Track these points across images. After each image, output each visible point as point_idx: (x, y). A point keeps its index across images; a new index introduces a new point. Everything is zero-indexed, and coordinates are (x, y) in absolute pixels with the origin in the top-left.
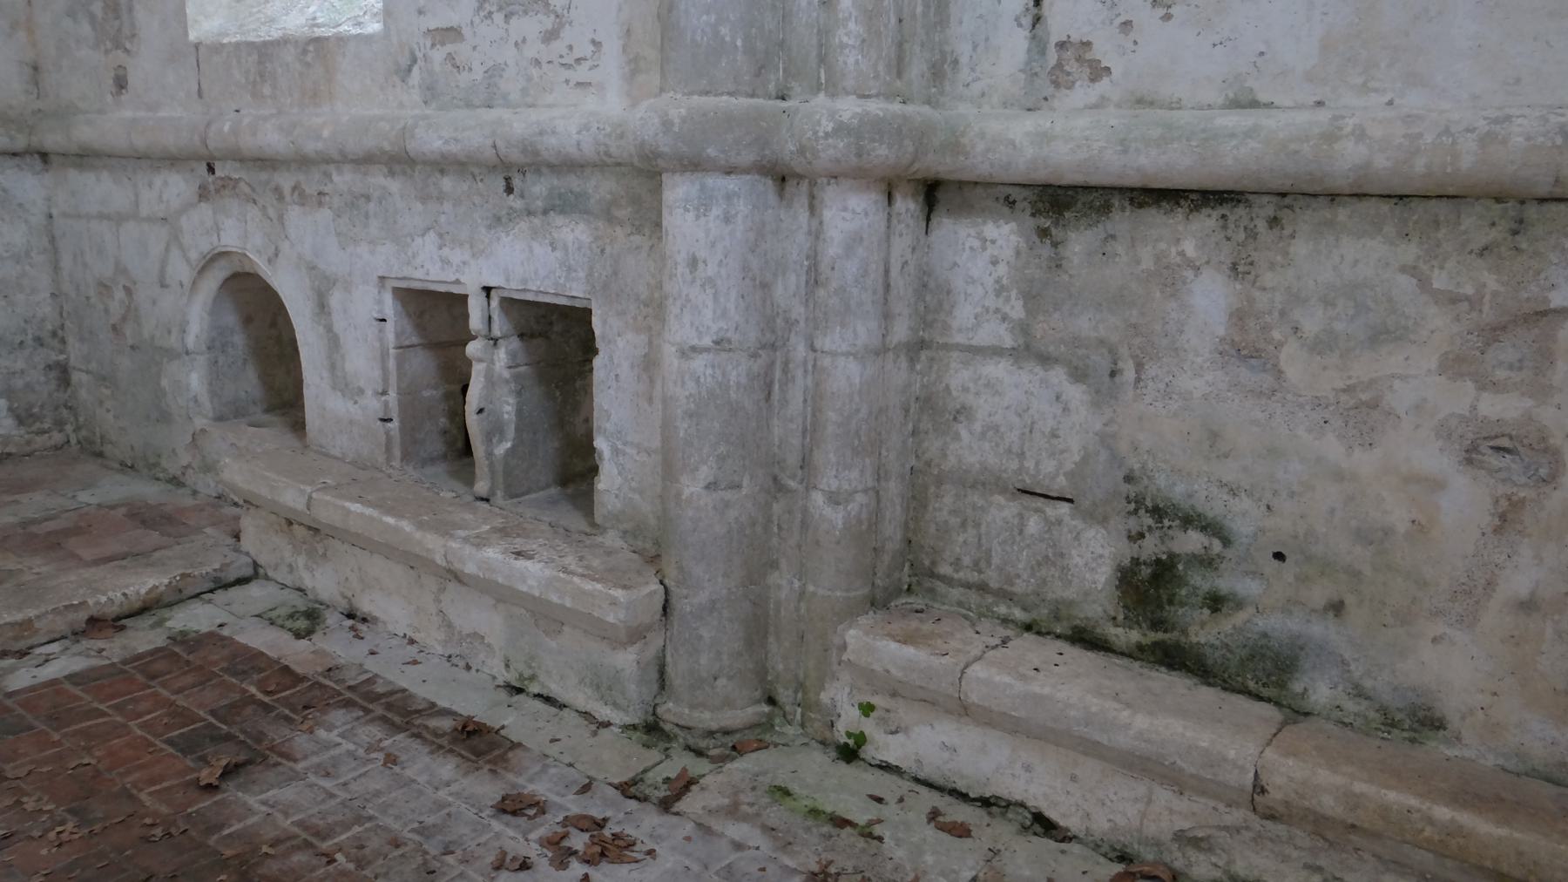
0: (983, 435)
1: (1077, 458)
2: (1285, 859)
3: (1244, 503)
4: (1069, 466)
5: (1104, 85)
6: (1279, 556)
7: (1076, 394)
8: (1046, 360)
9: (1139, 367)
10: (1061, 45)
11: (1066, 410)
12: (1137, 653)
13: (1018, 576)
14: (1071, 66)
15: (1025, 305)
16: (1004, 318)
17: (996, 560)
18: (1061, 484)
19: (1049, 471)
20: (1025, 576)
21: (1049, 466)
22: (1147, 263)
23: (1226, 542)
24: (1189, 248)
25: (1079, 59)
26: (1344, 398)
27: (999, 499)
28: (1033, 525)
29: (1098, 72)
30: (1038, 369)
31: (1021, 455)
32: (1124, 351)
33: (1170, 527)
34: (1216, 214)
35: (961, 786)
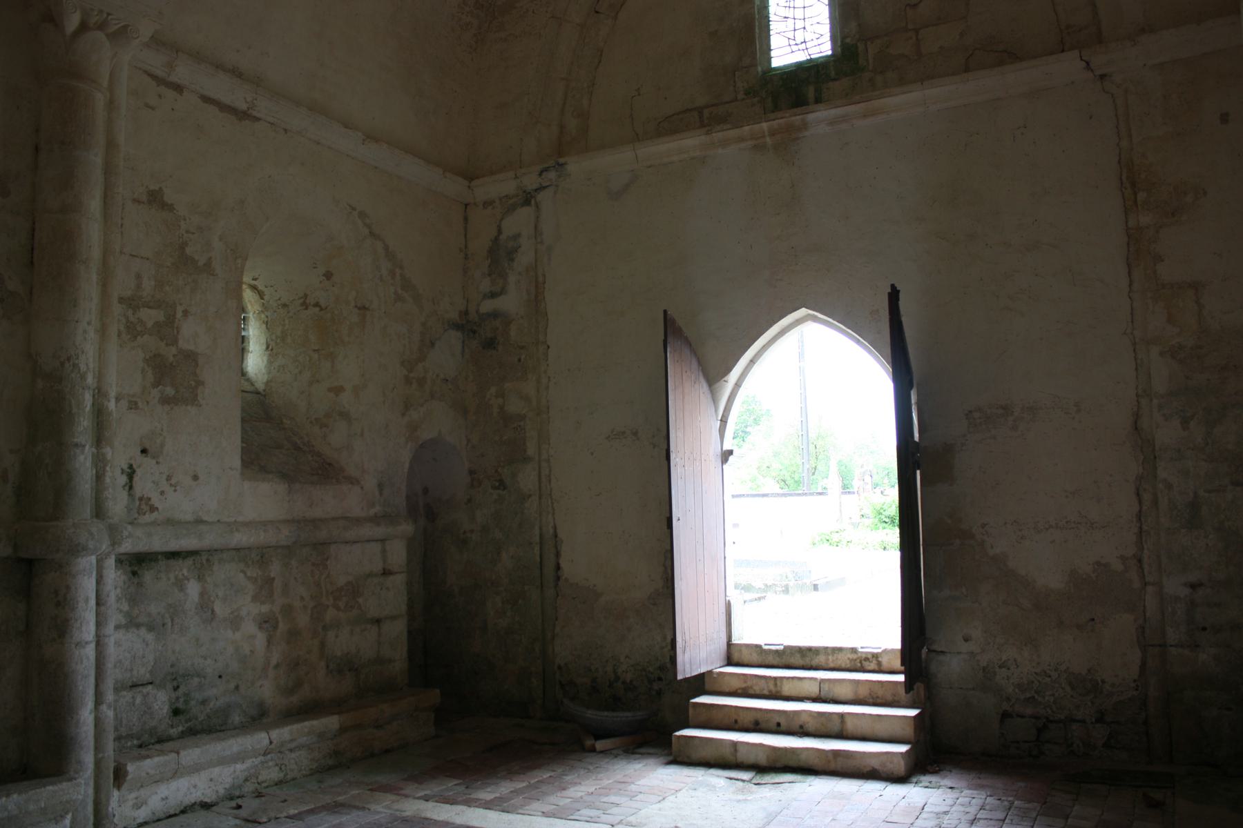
0: (115, 666)
1: (152, 664)
2: (269, 768)
3: (209, 661)
4: (150, 668)
5: (155, 514)
6: (220, 677)
7: (150, 637)
8: (138, 626)
9: (172, 620)
10: (141, 499)
11: (147, 645)
12: (182, 735)
13: (134, 725)
14: (143, 506)
15: (129, 605)
16: (121, 611)
17: (124, 722)
18: (148, 677)
19: (142, 673)
20: (136, 724)
21: (142, 671)
22: (173, 580)
23: (205, 677)
24: (185, 572)
25: (147, 504)
26: (231, 616)
27: (125, 693)
28: (138, 700)
29: (153, 509)
30: (135, 631)
31: (132, 670)
32: (167, 615)
33: (188, 679)
34: (192, 559)
35: (172, 812)
